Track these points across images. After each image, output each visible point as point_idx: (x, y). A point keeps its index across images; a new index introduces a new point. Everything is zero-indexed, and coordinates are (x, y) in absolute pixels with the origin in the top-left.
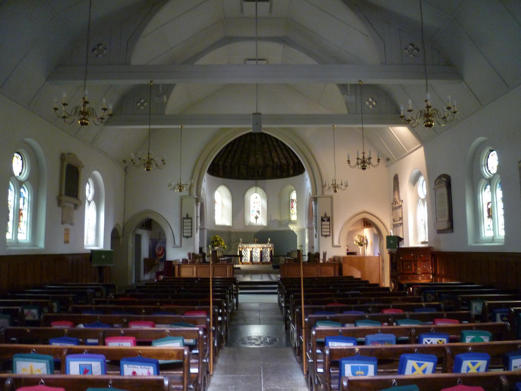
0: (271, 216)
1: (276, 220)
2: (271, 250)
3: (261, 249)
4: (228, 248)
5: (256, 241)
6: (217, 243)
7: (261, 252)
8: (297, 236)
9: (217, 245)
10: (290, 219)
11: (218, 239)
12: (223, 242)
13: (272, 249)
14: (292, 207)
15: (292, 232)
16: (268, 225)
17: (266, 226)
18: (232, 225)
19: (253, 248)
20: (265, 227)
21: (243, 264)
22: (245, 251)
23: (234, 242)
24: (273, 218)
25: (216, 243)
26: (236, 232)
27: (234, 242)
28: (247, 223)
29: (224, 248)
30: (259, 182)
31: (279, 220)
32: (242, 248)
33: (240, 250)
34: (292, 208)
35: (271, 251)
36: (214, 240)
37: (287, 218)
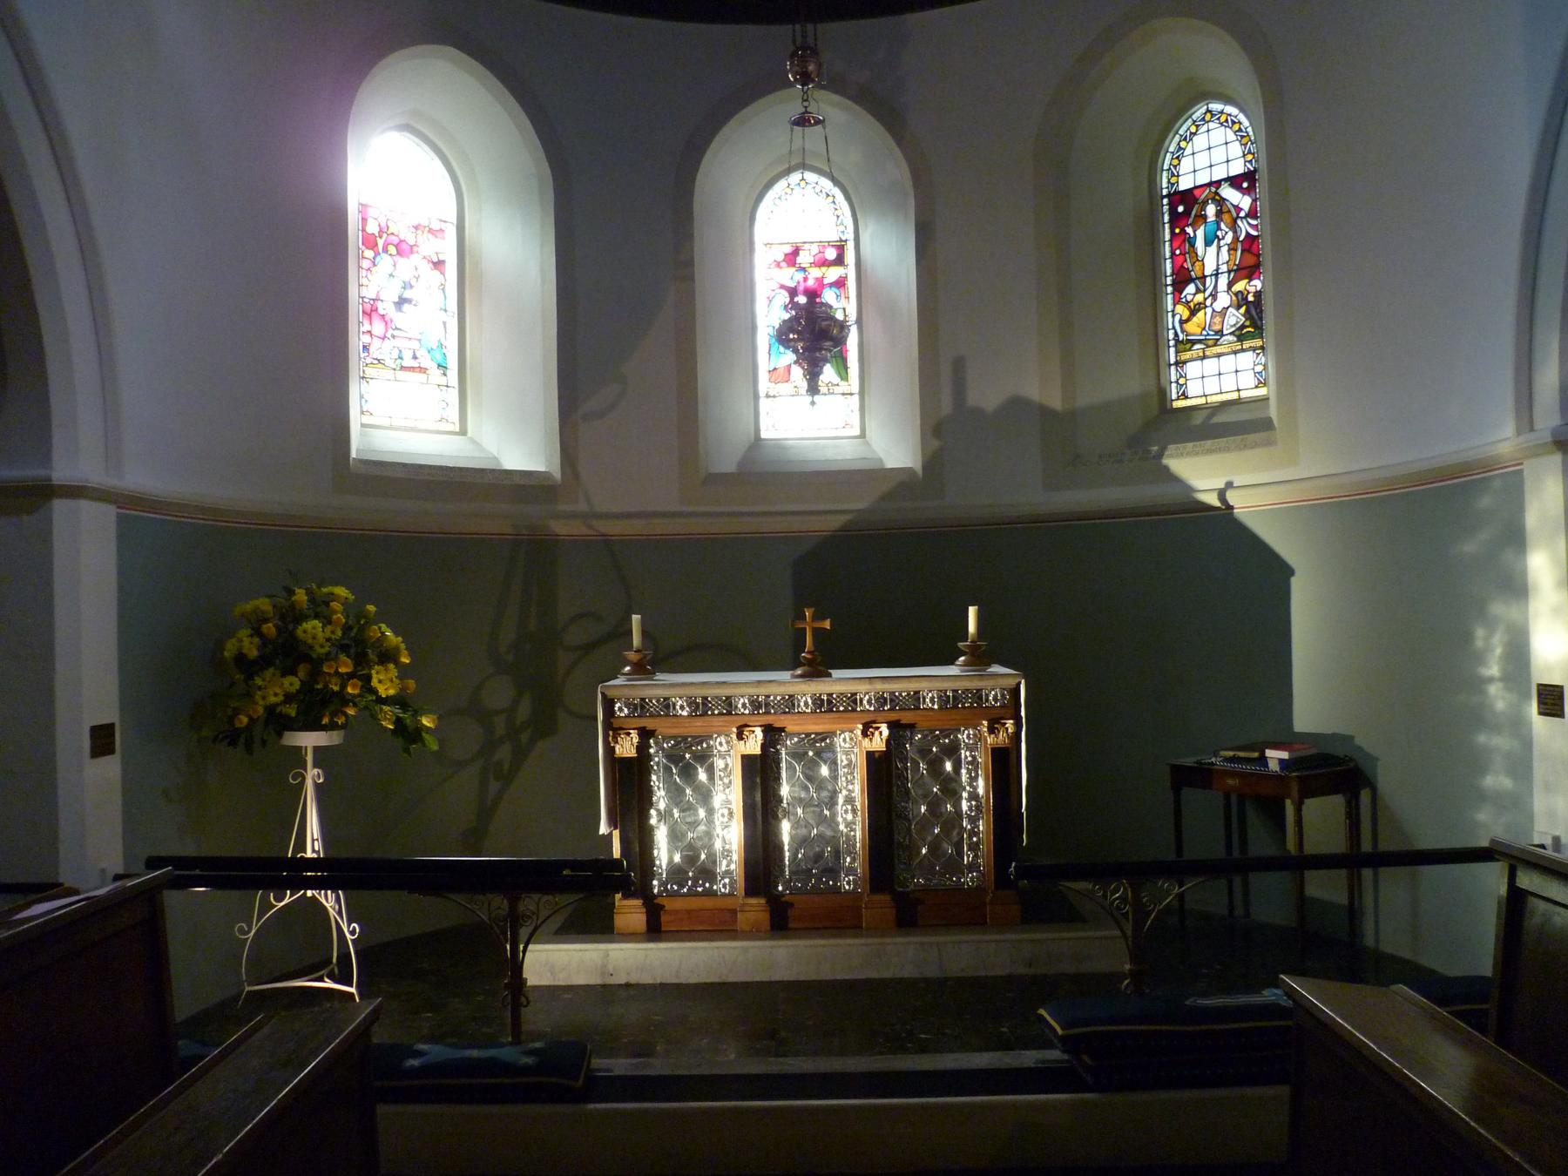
0: (959, 365)
1: (1017, 405)
2: (1002, 738)
3: (878, 742)
4: (524, 711)
5: (816, 631)
6: (293, 683)
7: (881, 771)
8: (1286, 571)
9: (292, 711)
10: (1163, 394)
11: (312, 628)
12: (387, 656)
13: (1016, 737)
14: (1182, 279)
15: (1223, 517)
16: (932, 463)
17: (908, 471)
18: (557, 474)
19: (773, 735)
20: (902, 483)
21: (655, 930)
22: (674, 757)
23: (588, 648)
24: (987, 395)
25: (276, 688)
26: (607, 544)
27: (588, 648)
28: (726, 463)
29: (408, 734)
30: (835, 35)
31: (1056, 402)
32: (645, 734)
33: (627, 747)
34: (1179, 286)
35: (1003, 761)
36: (251, 649)
37: (1125, 383)
